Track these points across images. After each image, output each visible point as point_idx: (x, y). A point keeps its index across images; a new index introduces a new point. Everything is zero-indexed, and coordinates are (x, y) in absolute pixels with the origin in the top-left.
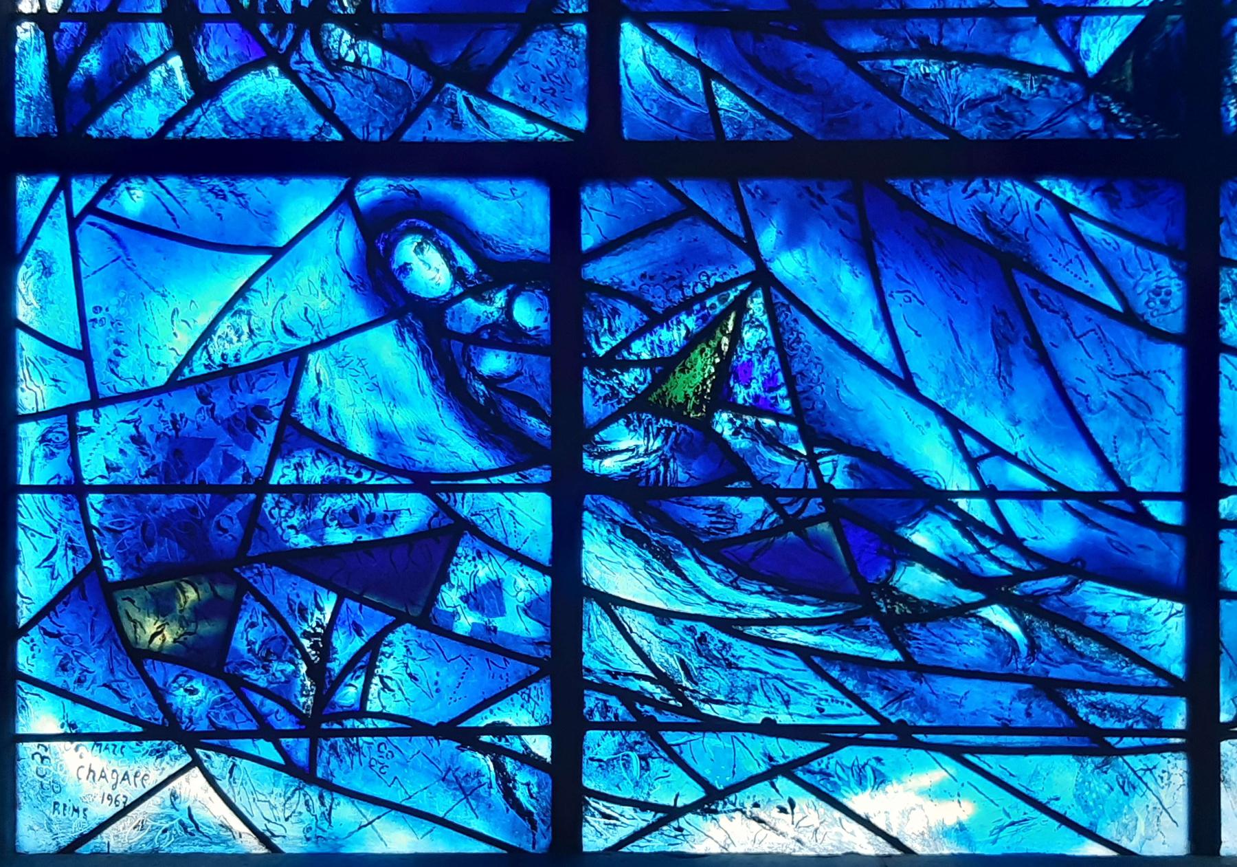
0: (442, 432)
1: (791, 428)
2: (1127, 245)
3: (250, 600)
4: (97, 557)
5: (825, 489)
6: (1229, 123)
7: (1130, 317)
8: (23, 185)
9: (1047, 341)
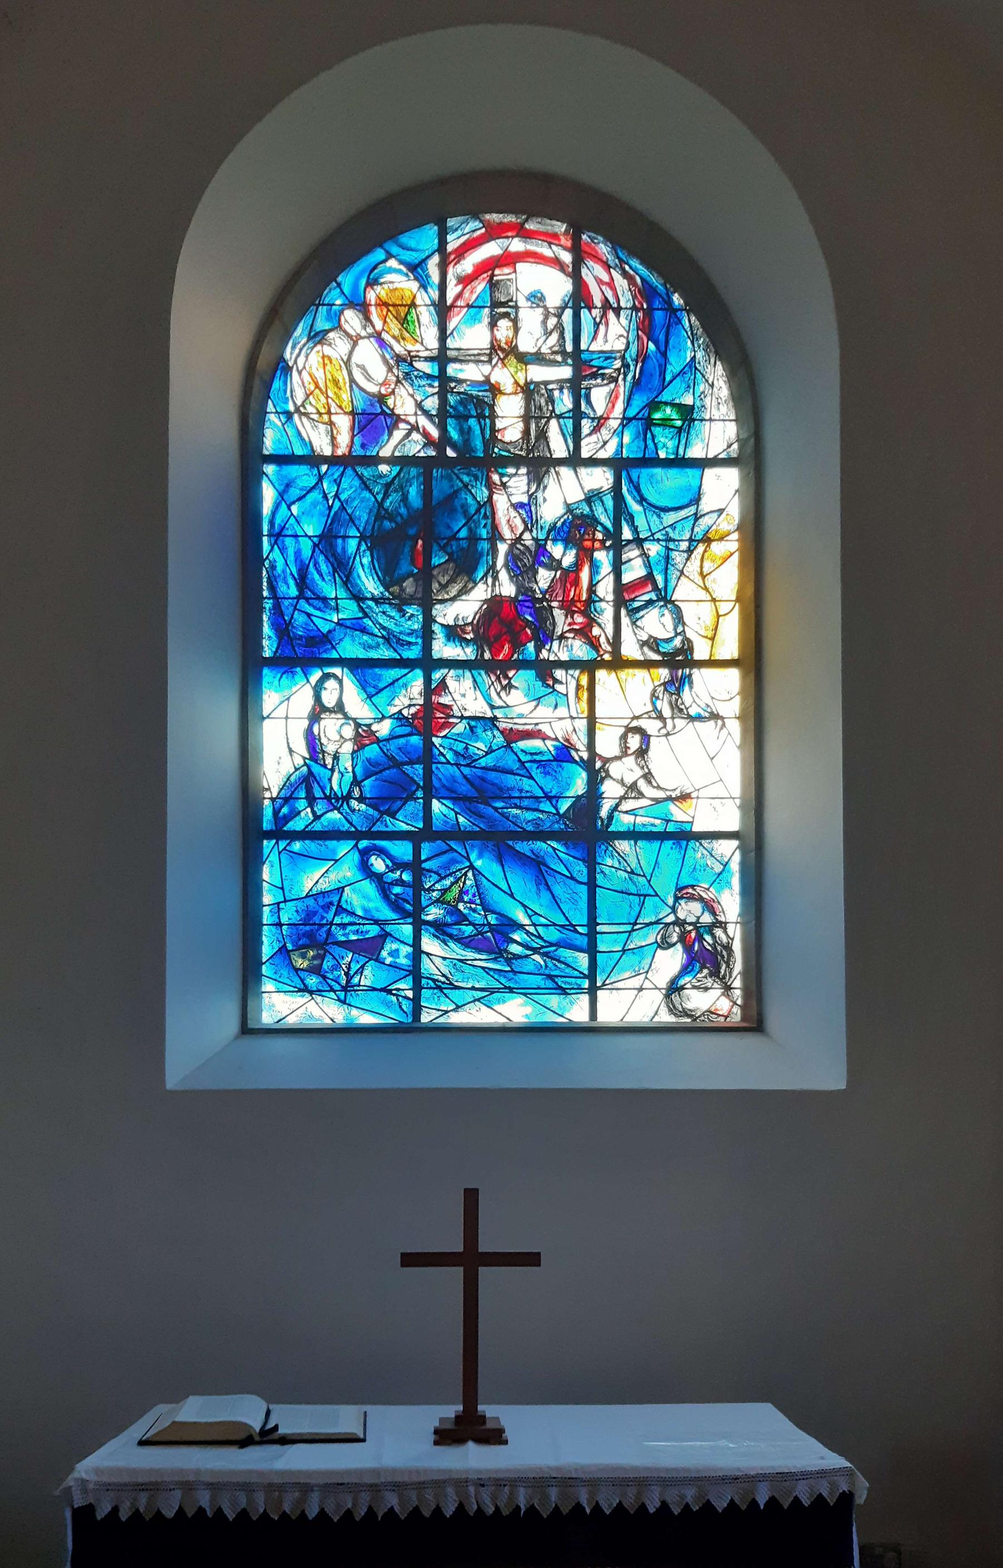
0: (382, 909)
1: (479, 907)
2: (571, 859)
3: (327, 954)
4: (285, 944)
5: (489, 924)
7: (572, 878)
8: (265, 842)
9: (550, 884)
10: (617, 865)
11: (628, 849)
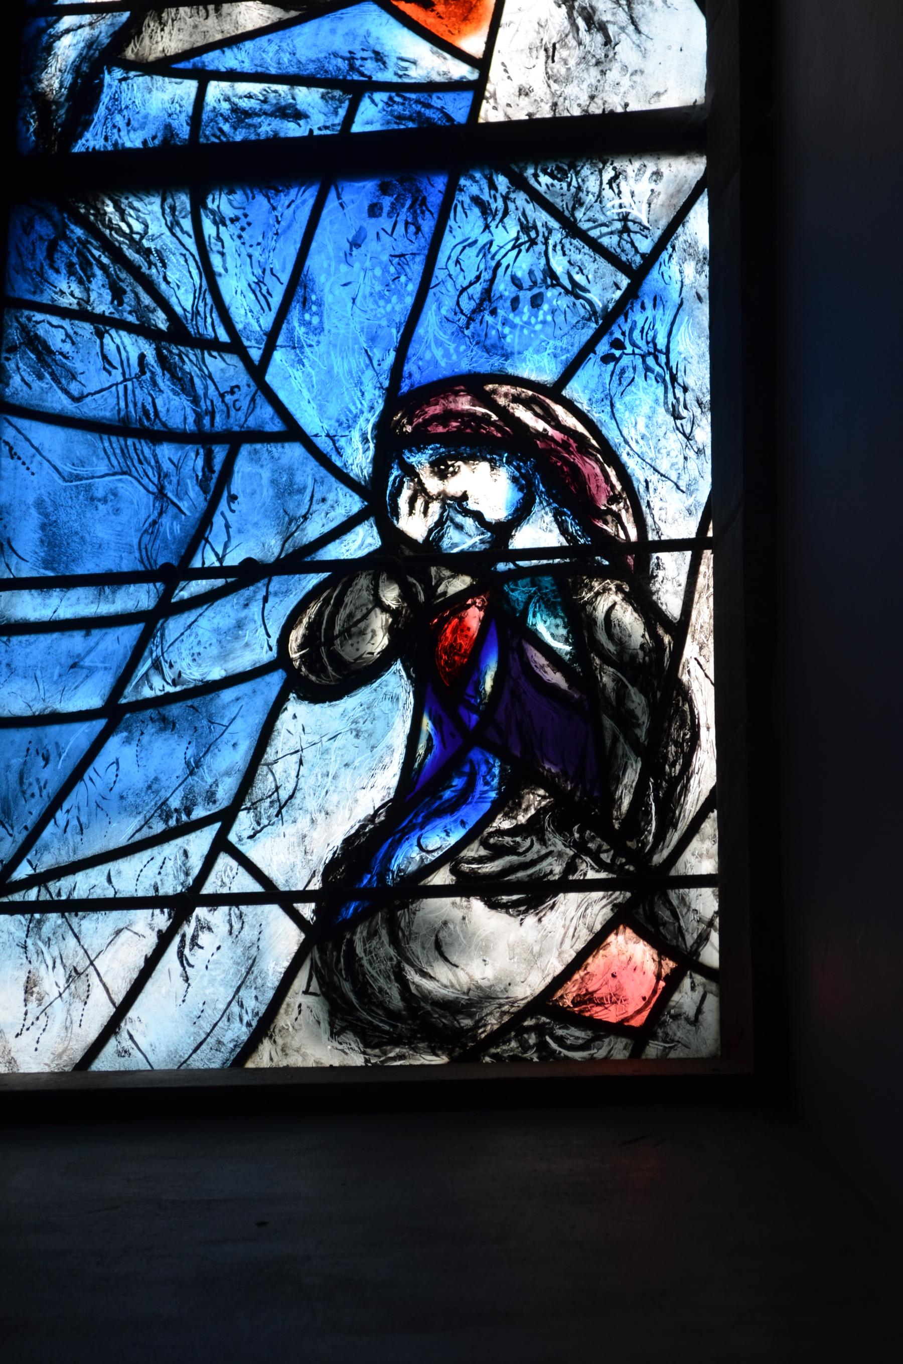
6: (28, 139)
10: (102, 304)
11: (157, 227)
